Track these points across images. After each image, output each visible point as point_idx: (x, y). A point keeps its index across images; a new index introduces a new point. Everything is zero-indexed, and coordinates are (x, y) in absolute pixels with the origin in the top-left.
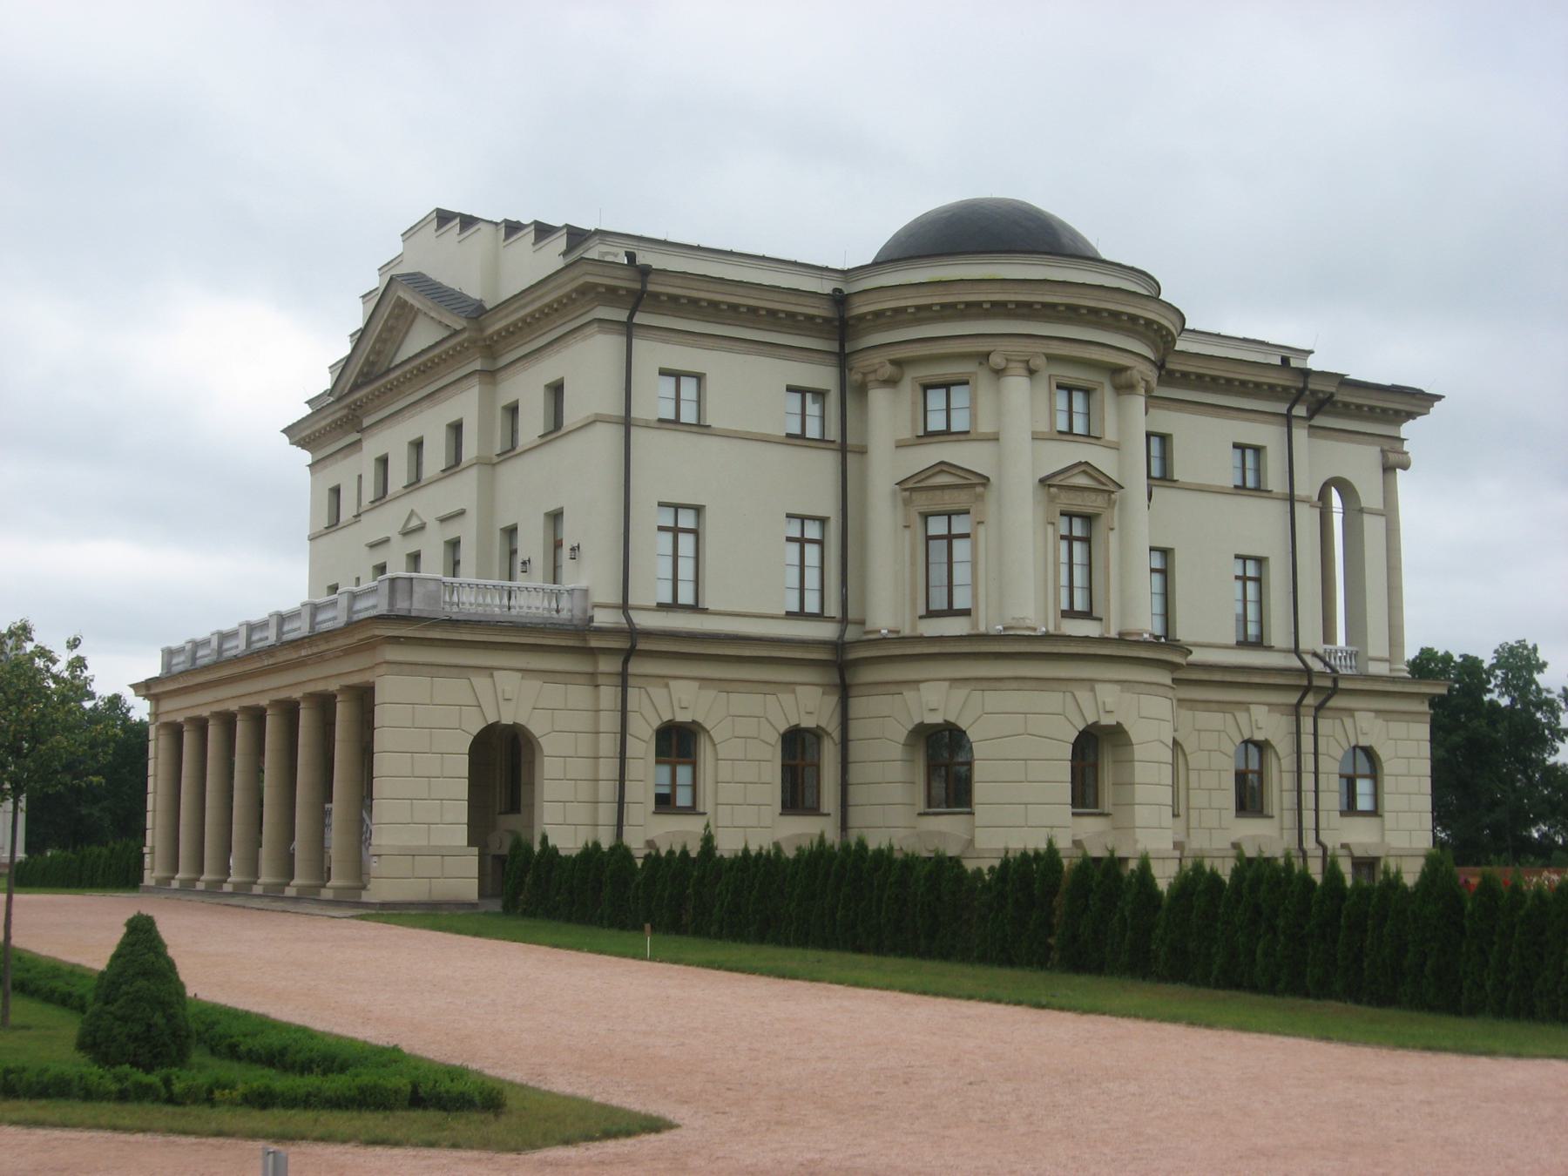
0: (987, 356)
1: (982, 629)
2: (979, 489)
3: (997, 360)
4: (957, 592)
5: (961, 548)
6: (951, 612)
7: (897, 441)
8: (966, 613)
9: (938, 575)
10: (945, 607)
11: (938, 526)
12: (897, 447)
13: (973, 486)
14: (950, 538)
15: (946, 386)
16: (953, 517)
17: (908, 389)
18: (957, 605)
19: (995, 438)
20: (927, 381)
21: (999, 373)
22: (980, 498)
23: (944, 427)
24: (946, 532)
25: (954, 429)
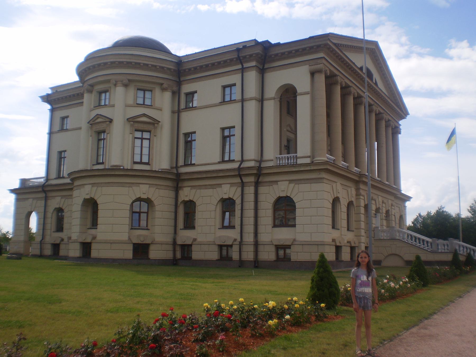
0: (162, 84)
2: (156, 125)
3: (165, 86)
5: (146, 143)
6: (141, 163)
9: (137, 150)
10: (139, 161)
11: (138, 134)
12: (126, 106)
14: (142, 139)
15: (144, 91)
16: (143, 133)
18: (143, 161)
19: (161, 110)
20: (140, 87)
21: (164, 90)
22: (155, 128)
24: (141, 137)
25: (145, 104)
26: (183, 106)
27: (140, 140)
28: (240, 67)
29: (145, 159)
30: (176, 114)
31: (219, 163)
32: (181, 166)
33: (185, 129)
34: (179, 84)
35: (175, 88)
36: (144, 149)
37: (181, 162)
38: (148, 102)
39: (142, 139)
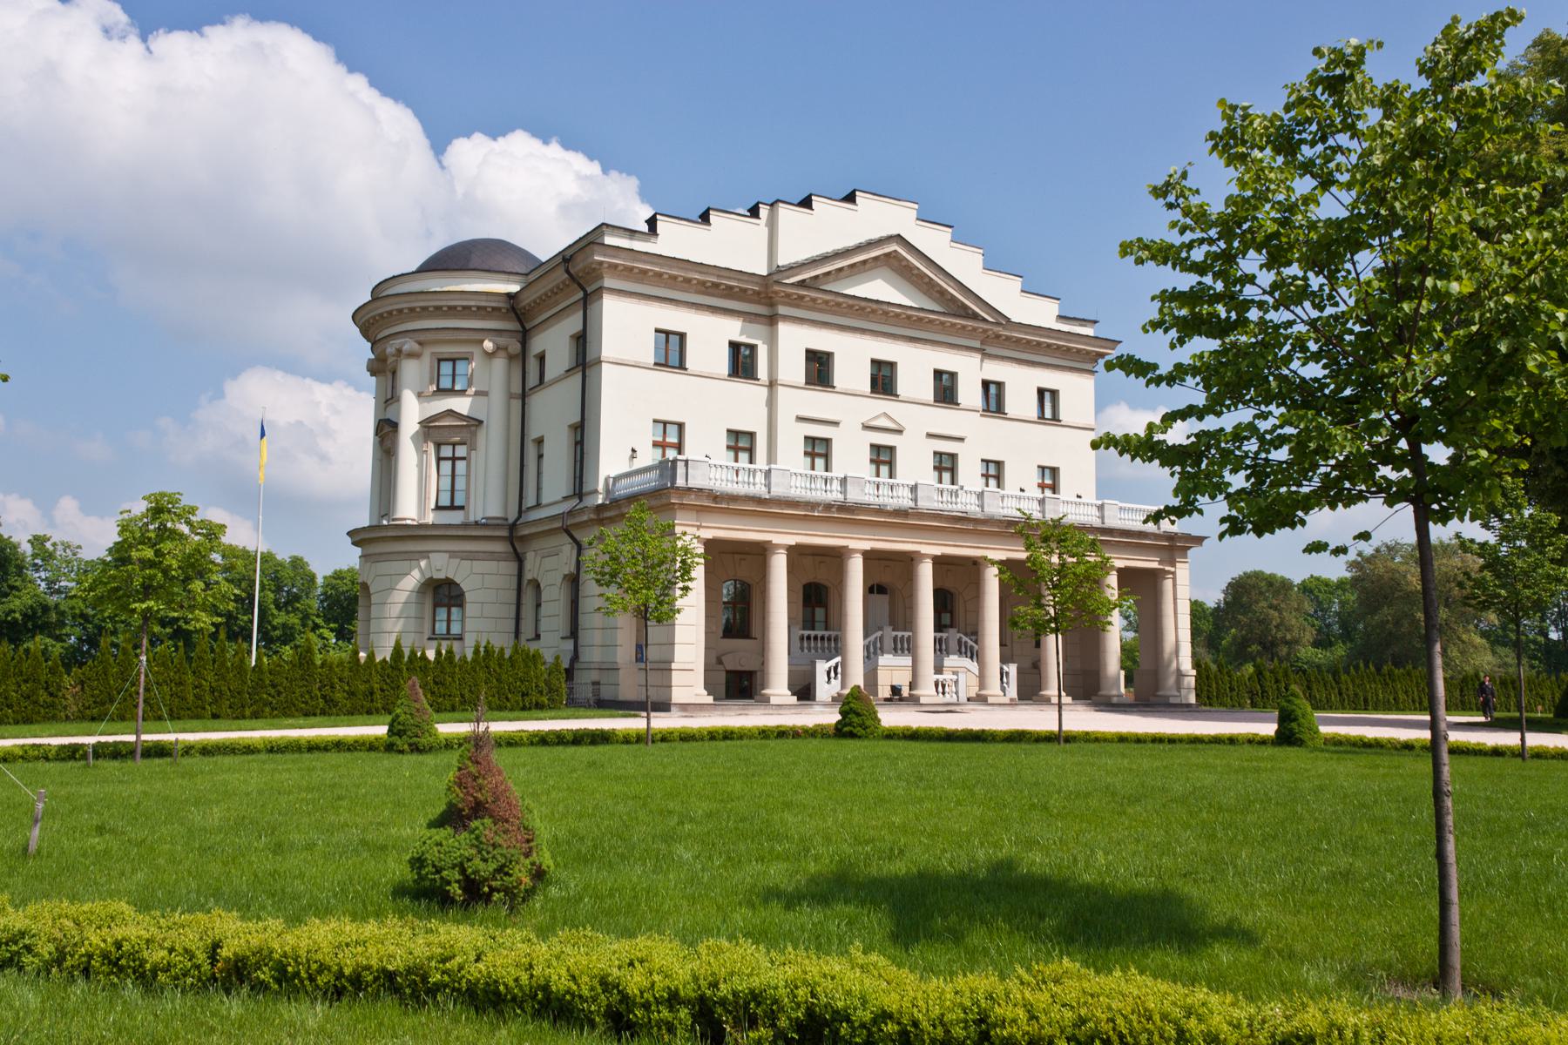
1: (472, 519)
4: (457, 495)
5: (461, 465)
6: (452, 507)
8: (462, 508)
11: (446, 451)
14: (454, 459)
15: (454, 360)
17: (427, 359)
18: (456, 504)
23: (449, 386)
26: (532, 379)
27: (450, 462)
28: (581, 294)
31: (566, 498)
32: (529, 509)
33: (533, 434)
34: (525, 336)
35: (515, 347)
36: (457, 479)
37: (530, 500)
39: (454, 459)
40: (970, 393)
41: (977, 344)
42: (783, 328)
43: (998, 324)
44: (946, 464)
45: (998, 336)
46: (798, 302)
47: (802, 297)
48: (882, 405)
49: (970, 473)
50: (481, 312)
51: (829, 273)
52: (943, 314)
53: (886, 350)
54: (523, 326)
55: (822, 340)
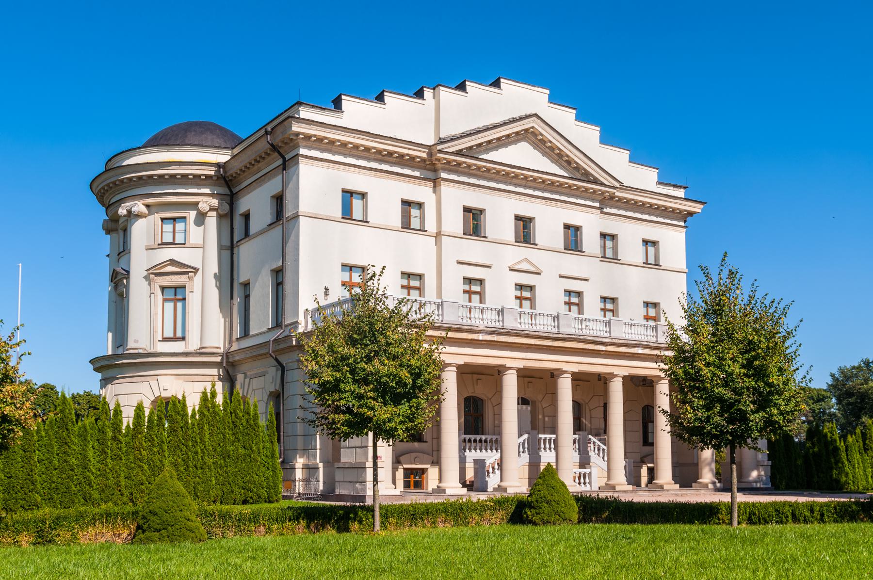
5: (179, 305)
7: (146, 246)
13: (187, 273)
23: (171, 241)
26: (238, 234)
28: (280, 161)
29: (179, 334)
30: (229, 253)
38: (179, 239)
40: (590, 241)
41: (597, 205)
42: (445, 188)
43: (614, 188)
44: (574, 299)
45: (612, 197)
46: (456, 168)
47: (459, 164)
48: (523, 252)
49: (592, 306)
50: (198, 180)
51: (480, 145)
52: (571, 178)
53: (526, 208)
54: (231, 191)
55: (475, 199)
